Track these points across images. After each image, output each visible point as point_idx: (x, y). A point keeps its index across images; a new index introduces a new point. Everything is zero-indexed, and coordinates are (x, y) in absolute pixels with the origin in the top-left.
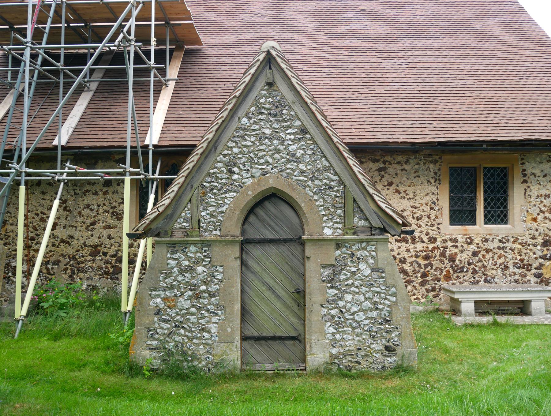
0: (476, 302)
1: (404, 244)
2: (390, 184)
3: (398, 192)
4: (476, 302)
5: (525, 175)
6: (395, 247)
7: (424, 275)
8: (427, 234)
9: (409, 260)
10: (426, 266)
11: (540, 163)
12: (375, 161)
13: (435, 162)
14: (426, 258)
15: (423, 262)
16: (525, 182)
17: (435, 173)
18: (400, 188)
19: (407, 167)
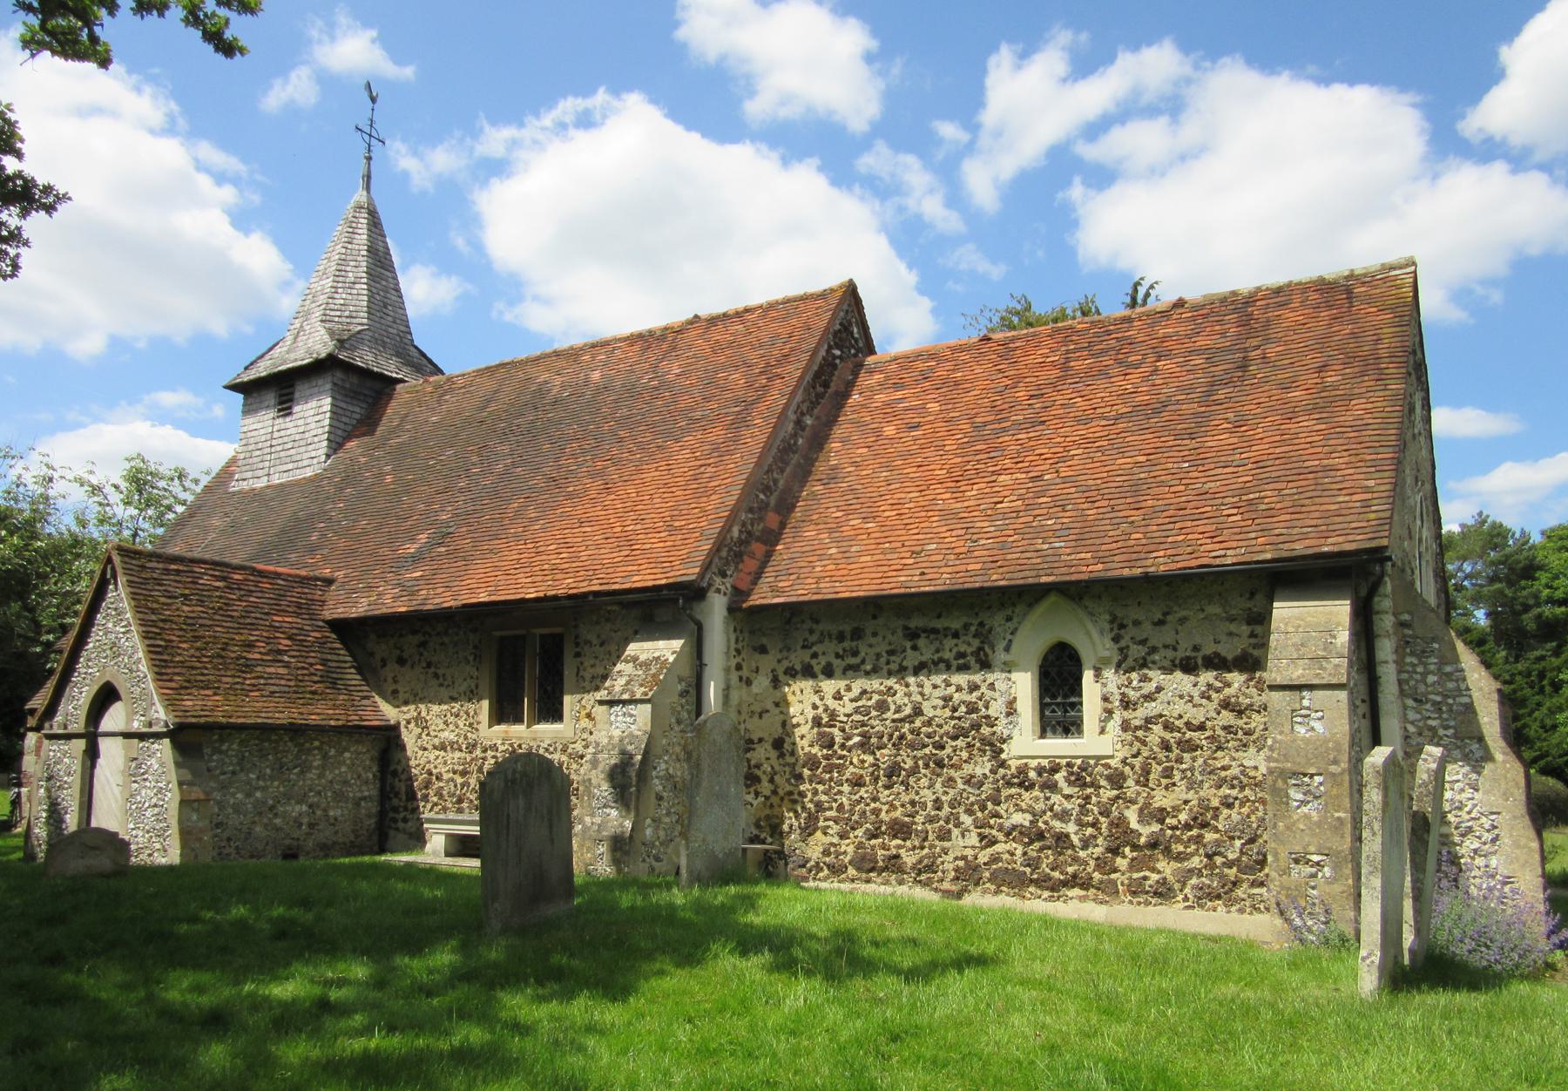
0: (448, 835)
1: (442, 753)
2: (429, 665)
3: (436, 676)
4: (448, 835)
5: (577, 645)
6: (432, 757)
7: (460, 801)
8: (466, 738)
9: (446, 776)
10: (463, 785)
11: (597, 623)
12: (414, 632)
13: (475, 631)
14: (464, 773)
15: (460, 780)
16: (578, 655)
17: (475, 647)
18: (440, 672)
19: (446, 640)
